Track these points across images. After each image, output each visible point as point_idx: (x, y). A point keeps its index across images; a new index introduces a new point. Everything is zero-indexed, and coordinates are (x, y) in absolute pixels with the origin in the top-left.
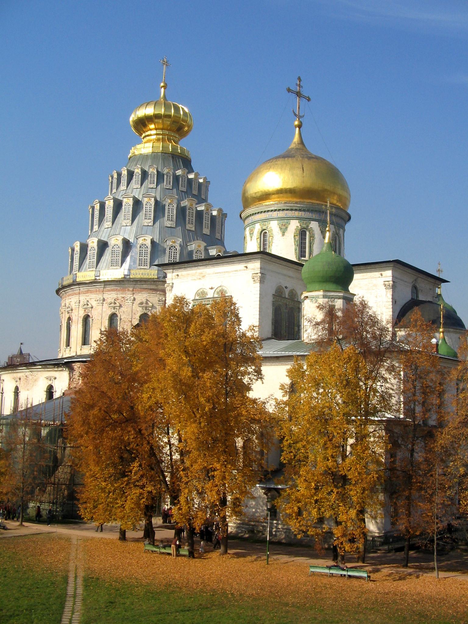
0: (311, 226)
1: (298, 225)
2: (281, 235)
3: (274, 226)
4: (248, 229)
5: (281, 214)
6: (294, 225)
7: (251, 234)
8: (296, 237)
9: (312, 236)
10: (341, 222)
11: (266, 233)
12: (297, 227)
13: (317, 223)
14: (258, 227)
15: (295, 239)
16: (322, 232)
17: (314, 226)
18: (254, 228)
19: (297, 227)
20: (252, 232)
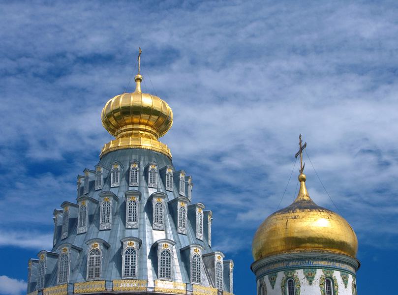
1: (322, 274)
4: (266, 278)
7: (273, 283)
8: (323, 286)
13: (339, 272)
15: (321, 288)
16: (344, 280)
17: (337, 275)
18: (276, 276)
20: (273, 281)
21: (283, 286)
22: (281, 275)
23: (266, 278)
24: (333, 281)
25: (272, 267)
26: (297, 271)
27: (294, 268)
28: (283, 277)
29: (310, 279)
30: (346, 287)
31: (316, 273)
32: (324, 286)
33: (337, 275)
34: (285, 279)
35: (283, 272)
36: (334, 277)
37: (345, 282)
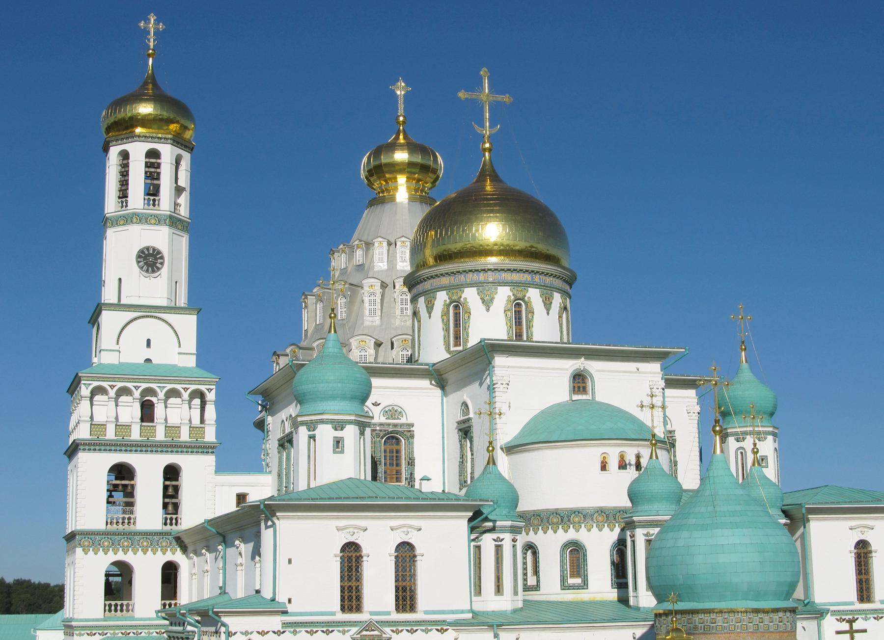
0: (527, 295)
1: (511, 294)
2: (484, 308)
4: (422, 300)
6: (504, 294)
7: (430, 309)
8: (509, 313)
9: (530, 311)
13: (538, 290)
16: (545, 304)
17: (534, 295)
20: (429, 306)
21: (445, 314)
22: (442, 297)
24: (526, 303)
25: (427, 285)
26: (466, 290)
27: (461, 287)
29: (487, 303)
30: (548, 313)
31: (497, 293)
34: (448, 301)
35: (445, 292)
36: (529, 298)
37: (548, 305)
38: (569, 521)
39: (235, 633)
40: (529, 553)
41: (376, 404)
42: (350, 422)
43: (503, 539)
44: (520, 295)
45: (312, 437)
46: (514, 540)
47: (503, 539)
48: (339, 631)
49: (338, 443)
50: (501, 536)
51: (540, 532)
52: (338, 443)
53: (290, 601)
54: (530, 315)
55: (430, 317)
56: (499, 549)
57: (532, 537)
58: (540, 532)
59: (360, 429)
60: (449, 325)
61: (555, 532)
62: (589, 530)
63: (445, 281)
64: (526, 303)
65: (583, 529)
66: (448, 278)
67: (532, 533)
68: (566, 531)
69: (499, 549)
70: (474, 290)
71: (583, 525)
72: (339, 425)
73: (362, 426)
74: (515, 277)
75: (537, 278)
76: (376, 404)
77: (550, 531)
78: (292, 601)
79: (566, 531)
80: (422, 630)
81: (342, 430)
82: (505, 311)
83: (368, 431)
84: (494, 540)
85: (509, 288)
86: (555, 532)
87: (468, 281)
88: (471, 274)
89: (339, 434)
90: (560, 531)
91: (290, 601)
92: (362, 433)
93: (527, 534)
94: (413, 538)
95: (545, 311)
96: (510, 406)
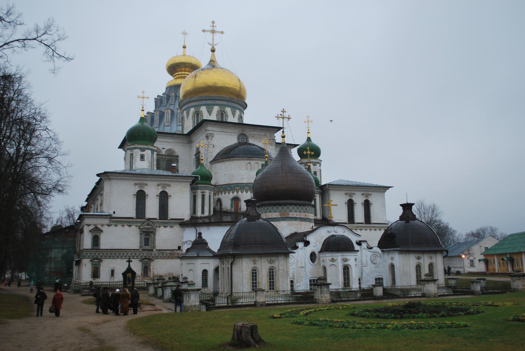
0: (226, 110)
1: (219, 109)
2: (208, 114)
3: (203, 109)
4: (185, 112)
5: (208, 102)
6: (216, 109)
8: (218, 116)
10: (242, 109)
11: (198, 114)
12: (218, 110)
13: (230, 108)
14: (192, 110)
15: (217, 117)
17: (228, 110)
18: (190, 111)
19: (218, 110)
21: (193, 116)
22: (192, 110)
23: (185, 112)
24: (225, 113)
26: (202, 107)
28: (194, 111)
29: (210, 113)
30: (234, 117)
32: (219, 116)
33: (228, 110)
35: (194, 108)
36: (226, 111)
37: (234, 114)
38: (234, 189)
39: (91, 225)
40: (219, 203)
41: (163, 149)
42: (149, 149)
43: (205, 192)
44: (222, 110)
45: (132, 155)
46: (210, 193)
47: (205, 192)
48: (135, 225)
49: (142, 157)
50: (204, 191)
51: (223, 194)
52: (142, 157)
53: (114, 213)
54: (226, 118)
55: (188, 118)
56: (203, 196)
57: (220, 196)
58: (223, 194)
59: (152, 152)
60: (195, 121)
61: (229, 193)
62: (242, 193)
63: (193, 104)
64: (225, 113)
65: (240, 193)
66: (195, 103)
67: (220, 194)
68: (233, 193)
69: (203, 196)
70: (205, 107)
71: (240, 191)
72: (143, 150)
73: (153, 151)
74: (220, 102)
75: (230, 104)
76: (163, 149)
77: (227, 193)
78: (116, 213)
79: (233, 193)
80: (170, 226)
81: (144, 151)
82: (217, 115)
83: (155, 153)
84: (201, 192)
85: (218, 107)
86: (229, 193)
87: (203, 103)
88: (204, 101)
89: (143, 153)
90: (231, 193)
91: (114, 213)
92: (152, 153)
93: (218, 195)
94: (168, 190)
95: (233, 116)
96: (213, 146)
